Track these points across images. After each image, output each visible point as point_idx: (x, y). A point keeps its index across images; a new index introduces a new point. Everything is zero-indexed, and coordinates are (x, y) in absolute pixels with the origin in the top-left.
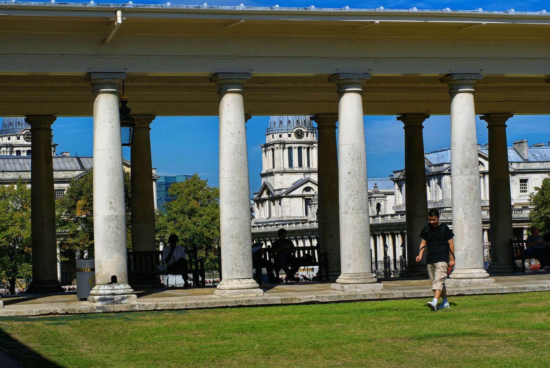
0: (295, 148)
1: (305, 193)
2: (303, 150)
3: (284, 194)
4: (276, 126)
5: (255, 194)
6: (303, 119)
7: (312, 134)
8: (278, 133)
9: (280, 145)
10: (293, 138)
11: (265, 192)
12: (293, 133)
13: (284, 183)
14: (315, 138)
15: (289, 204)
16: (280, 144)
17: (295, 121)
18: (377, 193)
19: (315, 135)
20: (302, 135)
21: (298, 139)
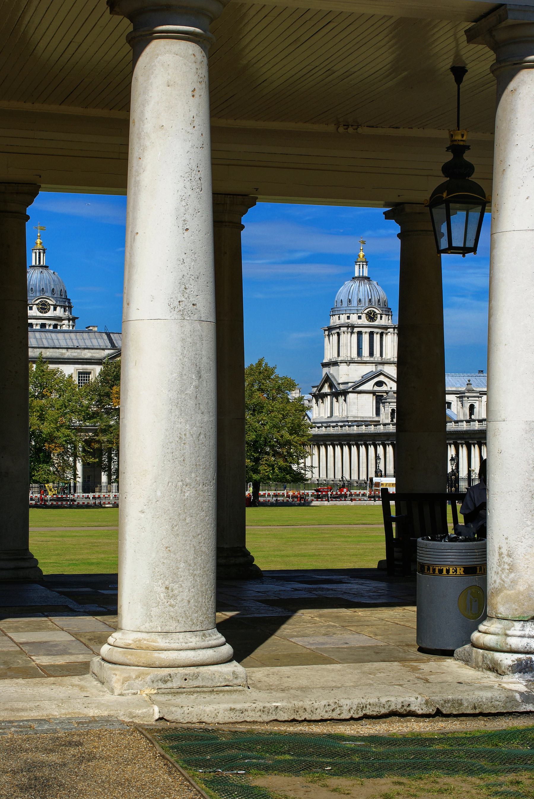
0: (366, 333)
1: (376, 388)
2: (375, 335)
3: (351, 389)
4: (343, 306)
5: (313, 387)
6: (376, 298)
8: (346, 314)
9: (348, 329)
10: (364, 321)
11: (326, 386)
13: (350, 376)
14: (390, 321)
15: (356, 401)
16: (348, 327)
17: (367, 300)
18: (470, 392)
19: (390, 318)
20: (374, 317)
21: (370, 321)
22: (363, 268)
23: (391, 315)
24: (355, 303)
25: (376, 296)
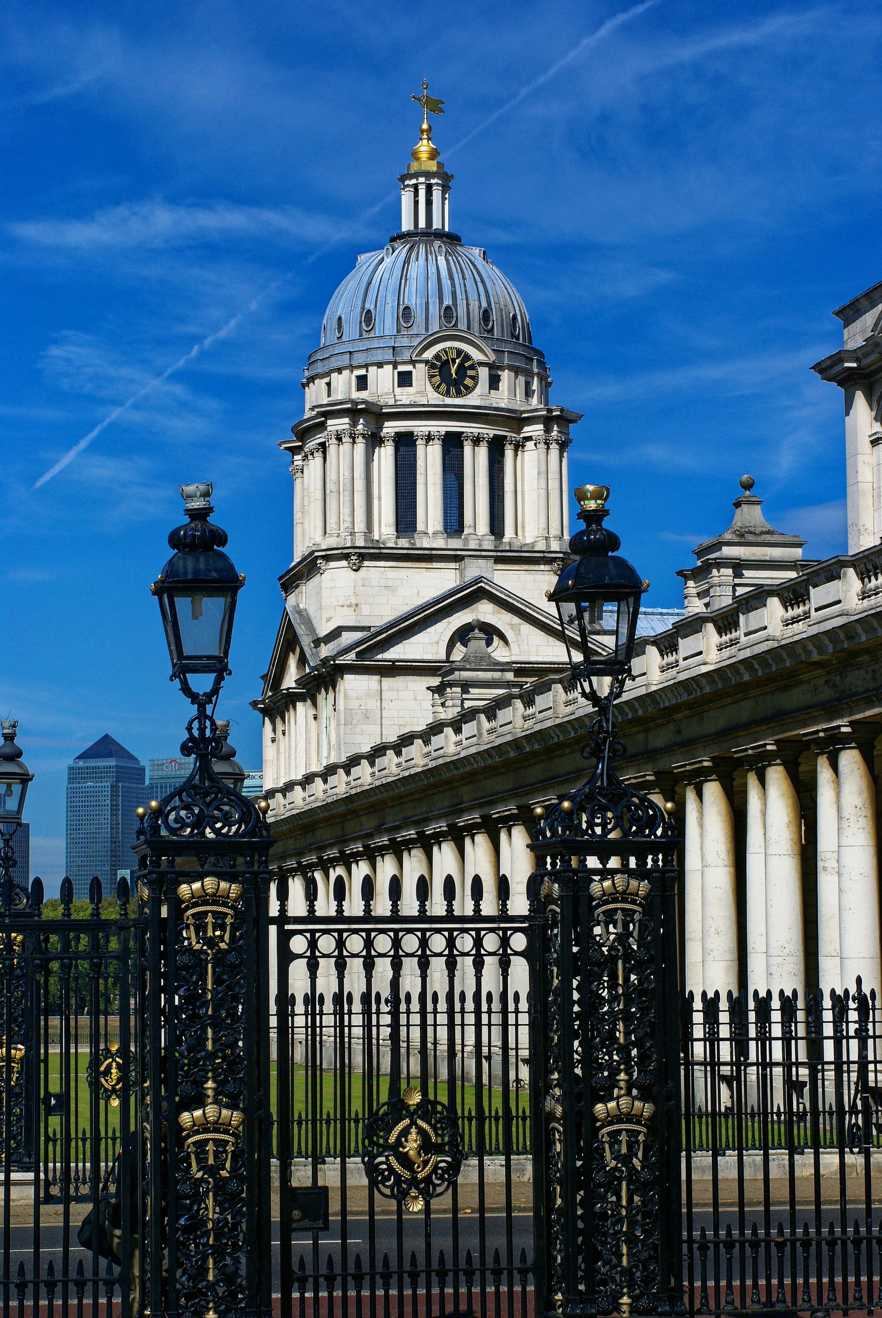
0: (429, 438)
2: (468, 449)
3: (352, 656)
4: (344, 338)
6: (474, 306)
7: (521, 379)
8: (352, 368)
9: (354, 424)
12: (421, 367)
13: (365, 610)
14: (535, 401)
15: (373, 704)
17: (435, 311)
18: (750, 538)
19: (535, 386)
21: (448, 394)
22: (429, 203)
23: (542, 378)
24: (387, 323)
25: (473, 296)
